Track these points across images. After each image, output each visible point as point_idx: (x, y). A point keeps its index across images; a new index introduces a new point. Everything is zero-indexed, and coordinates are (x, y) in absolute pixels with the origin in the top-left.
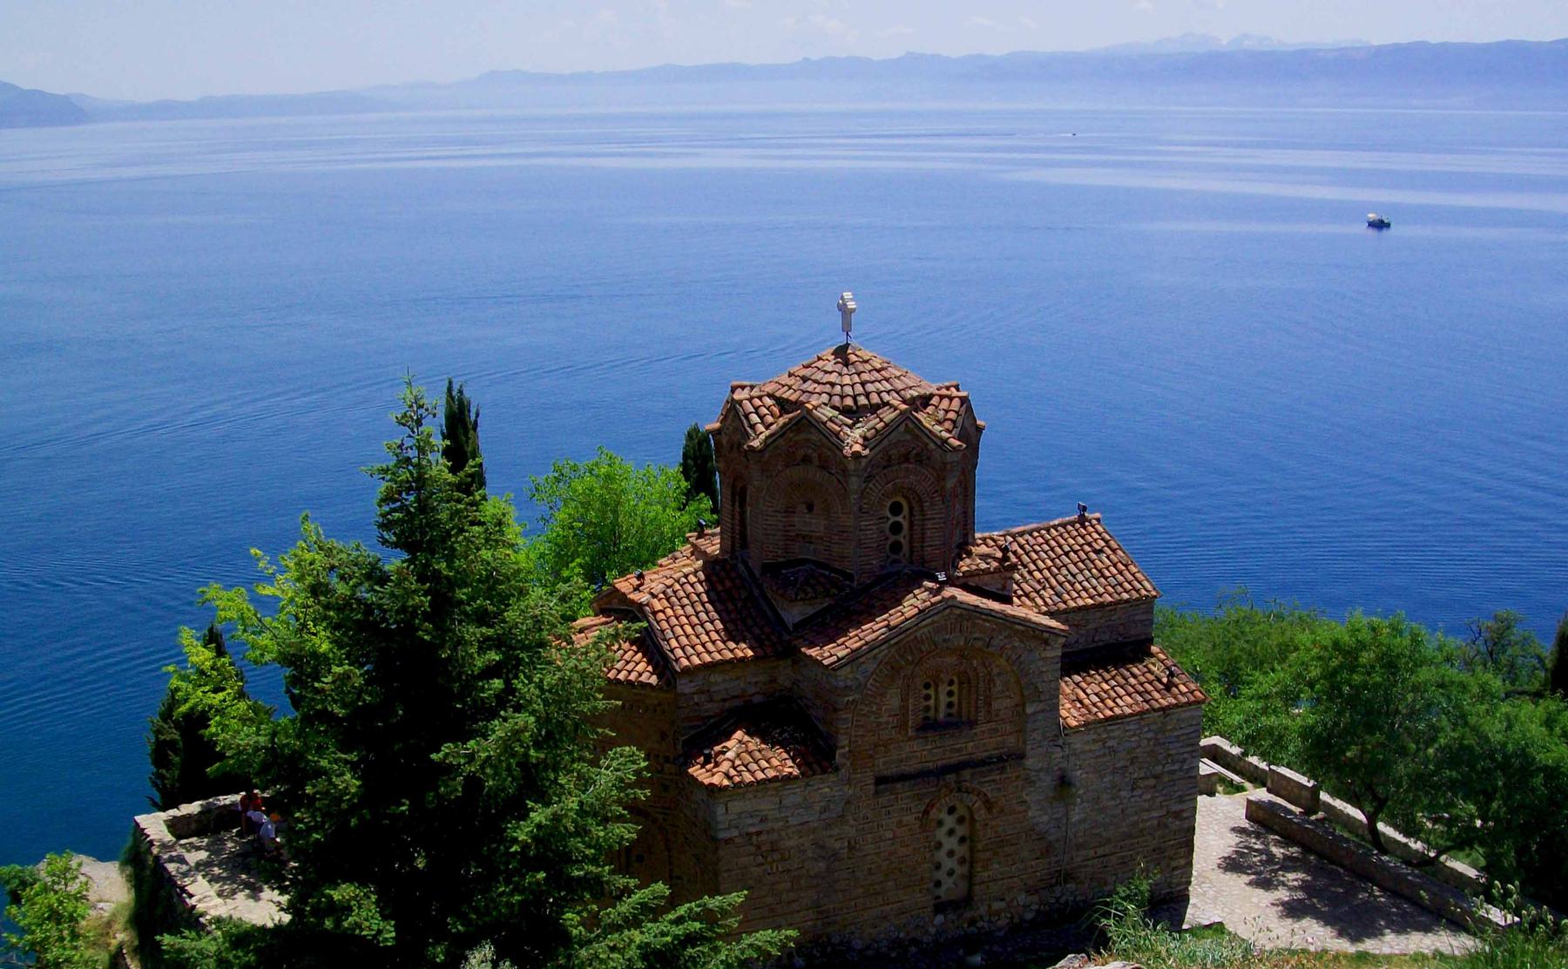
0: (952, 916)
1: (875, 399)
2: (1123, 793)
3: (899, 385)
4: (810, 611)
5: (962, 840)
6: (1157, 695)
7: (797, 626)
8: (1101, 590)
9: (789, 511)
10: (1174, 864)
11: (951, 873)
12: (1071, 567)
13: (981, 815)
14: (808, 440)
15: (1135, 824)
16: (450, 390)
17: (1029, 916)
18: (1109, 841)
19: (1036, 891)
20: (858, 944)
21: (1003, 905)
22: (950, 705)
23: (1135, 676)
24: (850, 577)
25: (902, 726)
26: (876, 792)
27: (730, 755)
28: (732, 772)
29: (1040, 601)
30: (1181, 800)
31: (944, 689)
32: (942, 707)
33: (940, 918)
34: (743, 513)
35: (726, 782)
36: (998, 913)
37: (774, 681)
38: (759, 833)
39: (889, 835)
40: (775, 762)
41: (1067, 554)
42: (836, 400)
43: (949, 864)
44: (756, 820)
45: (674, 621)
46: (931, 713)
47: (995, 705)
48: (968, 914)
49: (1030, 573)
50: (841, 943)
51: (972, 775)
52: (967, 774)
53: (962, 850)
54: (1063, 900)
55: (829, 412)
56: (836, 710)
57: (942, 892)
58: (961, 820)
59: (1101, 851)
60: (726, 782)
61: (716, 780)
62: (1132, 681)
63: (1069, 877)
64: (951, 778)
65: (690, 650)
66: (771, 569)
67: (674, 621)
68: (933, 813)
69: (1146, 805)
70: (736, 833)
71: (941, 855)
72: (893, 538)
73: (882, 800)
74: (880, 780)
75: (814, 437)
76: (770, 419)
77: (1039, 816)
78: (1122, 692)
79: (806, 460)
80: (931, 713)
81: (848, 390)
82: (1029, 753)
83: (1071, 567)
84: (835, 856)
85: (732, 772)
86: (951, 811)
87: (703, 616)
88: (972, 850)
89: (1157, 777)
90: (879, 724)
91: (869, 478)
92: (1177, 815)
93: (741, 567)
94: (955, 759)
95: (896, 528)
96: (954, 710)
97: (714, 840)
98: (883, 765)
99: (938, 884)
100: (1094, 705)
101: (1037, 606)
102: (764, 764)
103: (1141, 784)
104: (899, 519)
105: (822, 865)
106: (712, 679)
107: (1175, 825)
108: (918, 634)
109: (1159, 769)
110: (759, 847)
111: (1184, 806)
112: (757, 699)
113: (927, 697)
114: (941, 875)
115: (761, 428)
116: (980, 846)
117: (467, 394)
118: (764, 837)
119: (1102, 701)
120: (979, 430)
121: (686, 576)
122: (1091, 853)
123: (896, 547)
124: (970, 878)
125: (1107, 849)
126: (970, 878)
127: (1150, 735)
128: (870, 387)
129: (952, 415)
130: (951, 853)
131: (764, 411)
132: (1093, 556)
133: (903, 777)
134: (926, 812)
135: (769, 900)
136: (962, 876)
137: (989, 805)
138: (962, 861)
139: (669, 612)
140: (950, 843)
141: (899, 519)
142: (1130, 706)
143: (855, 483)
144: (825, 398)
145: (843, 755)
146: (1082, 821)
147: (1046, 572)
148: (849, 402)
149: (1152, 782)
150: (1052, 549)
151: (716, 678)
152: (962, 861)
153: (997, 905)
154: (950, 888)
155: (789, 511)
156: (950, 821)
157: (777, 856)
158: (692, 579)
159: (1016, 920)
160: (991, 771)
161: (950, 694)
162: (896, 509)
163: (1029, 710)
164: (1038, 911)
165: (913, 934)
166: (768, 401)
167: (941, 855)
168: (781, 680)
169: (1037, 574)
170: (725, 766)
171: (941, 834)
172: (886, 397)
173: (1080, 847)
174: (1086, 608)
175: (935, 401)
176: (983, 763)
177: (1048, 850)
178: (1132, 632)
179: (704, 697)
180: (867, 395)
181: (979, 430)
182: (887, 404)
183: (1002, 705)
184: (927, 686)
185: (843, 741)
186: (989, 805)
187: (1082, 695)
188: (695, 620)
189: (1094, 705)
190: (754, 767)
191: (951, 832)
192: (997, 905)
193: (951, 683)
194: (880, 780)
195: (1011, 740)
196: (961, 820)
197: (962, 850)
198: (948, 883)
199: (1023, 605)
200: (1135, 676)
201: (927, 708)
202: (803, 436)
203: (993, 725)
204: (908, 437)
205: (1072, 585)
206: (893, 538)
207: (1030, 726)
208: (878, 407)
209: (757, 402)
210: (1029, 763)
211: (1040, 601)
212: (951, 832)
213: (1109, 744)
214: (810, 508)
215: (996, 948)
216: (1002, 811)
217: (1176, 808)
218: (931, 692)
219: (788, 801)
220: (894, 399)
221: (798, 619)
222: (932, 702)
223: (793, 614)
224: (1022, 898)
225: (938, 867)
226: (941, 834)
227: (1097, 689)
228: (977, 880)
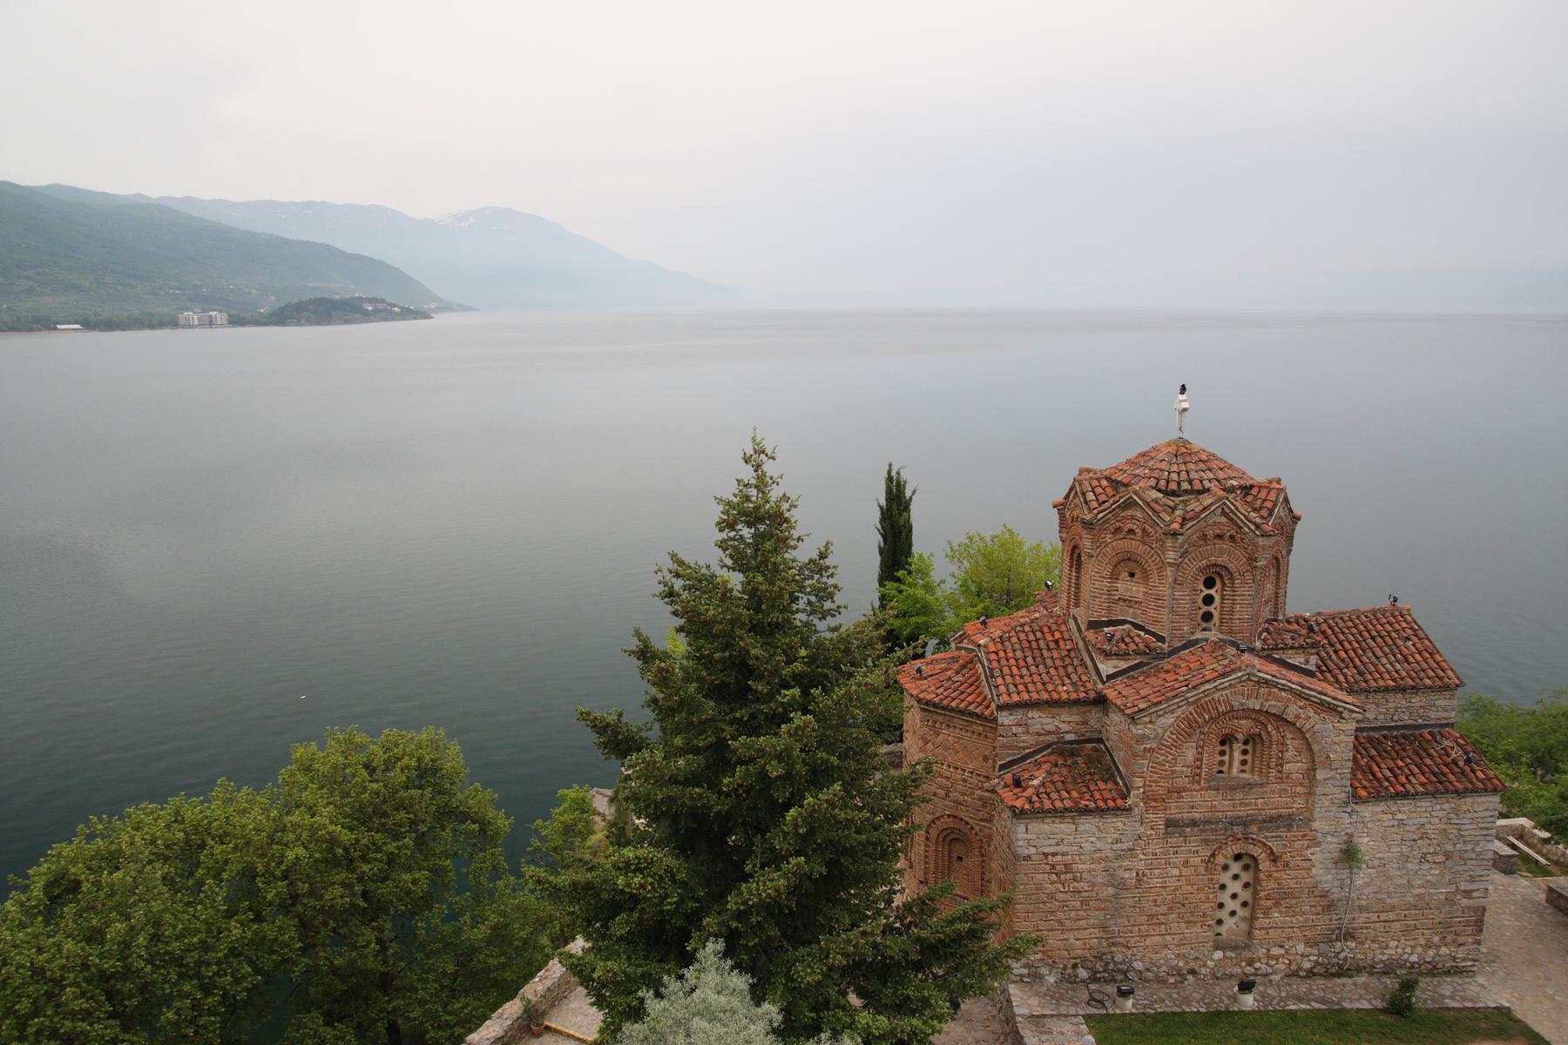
0: (1229, 954)
1: (1197, 486)
2: (1410, 866)
3: (1221, 475)
4: (1123, 665)
5: (1246, 885)
6: (1452, 777)
7: (1110, 677)
8: (1404, 674)
9: (1114, 577)
10: (1461, 940)
11: (1233, 913)
12: (1377, 651)
13: (1265, 865)
14: (1133, 517)
15: (1420, 896)
16: (889, 472)
17: (1307, 965)
18: (1393, 908)
19: (1316, 944)
20: (1138, 965)
21: (1282, 951)
22: (1244, 762)
23: (1429, 755)
24: (1162, 639)
25: (1195, 777)
26: (1167, 833)
27: (1035, 782)
28: (1035, 798)
29: (1342, 678)
30: (1472, 880)
31: (1238, 747)
32: (1236, 763)
33: (1218, 955)
34: (1078, 578)
35: (1027, 806)
36: (1277, 958)
37: (1085, 723)
38: (1054, 855)
39: (1176, 872)
40: (1075, 794)
41: (1373, 638)
42: (1163, 483)
43: (1231, 905)
44: (1053, 842)
45: (1003, 662)
46: (1225, 769)
47: (1287, 767)
48: (1246, 954)
49: (1336, 652)
50: (1124, 962)
51: (1260, 829)
52: (1254, 828)
53: (1245, 895)
54: (1342, 956)
55: (1155, 494)
56: (1135, 755)
57: (1223, 929)
58: (1246, 868)
59: (1383, 917)
60: (1027, 806)
61: (1018, 803)
62: (1428, 761)
63: (1349, 935)
64: (1238, 830)
65: (1012, 689)
66: (1095, 625)
67: (1003, 662)
68: (1220, 860)
69: (1433, 879)
70: (1033, 850)
71: (1225, 897)
72: (1205, 608)
73: (1173, 840)
74: (1170, 823)
75: (1139, 515)
76: (1102, 498)
77: (1323, 873)
78: (1416, 771)
79: (1131, 531)
80: (1225, 769)
81: (1175, 476)
82: (1317, 815)
83: (1377, 651)
84: (1122, 886)
85: (1035, 798)
86: (1238, 857)
87: (1030, 660)
88: (1255, 894)
89: (1448, 855)
90: (1173, 772)
91: (1184, 554)
92: (1468, 894)
93: (1071, 621)
94: (1242, 812)
95: (1208, 600)
96: (1247, 768)
97: (1015, 855)
98: (1176, 809)
99: (1220, 922)
100: (1387, 779)
101: (1337, 681)
102: (1064, 794)
103: (1429, 857)
104: (1212, 592)
105: (1111, 890)
106: (1030, 714)
107: (1465, 901)
108: (1216, 696)
109: (1449, 847)
110: (1053, 867)
111: (1473, 887)
112: (1069, 737)
113: (1222, 753)
114: (1224, 915)
115: (1095, 504)
116: (1262, 894)
117: (904, 476)
118: (1059, 858)
119: (1395, 776)
120: (1296, 519)
121: (1023, 625)
122: (1374, 917)
123: (1207, 617)
124: (1251, 919)
125: (1391, 916)
126: (1251, 919)
127: (1442, 814)
128: (1193, 475)
129: (1269, 505)
130: (1234, 896)
131: (1099, 490)
132: (1400, 643)
133: (1194, 823)
134: (1213, 855)
135: (1060, 915)
136: (1243, 919)
137: (1274, 858)
138: (1245, 904)
139: (1002, 654)
140: (1235, 887)
141: (1212, 592)
142: (1422, 784)
143: (1171, 556)
144: (1153, 482)
145: (1137, 796)
146: (1368, 885)
147: (1351, 653)
148: (1173, 486)
149: (1441, 858)
150: (1360, 633)
151: (1034, 714)
152: (1245, 904)
153: (1276, 951)
155: (1114, 577)
156: (1235, 868)
157: (1069, 876)
158: (1027, 628)
159: (1293, 967)
160: (1278, 827)
161: (1245, 752)
162: (1209, 583)
163: (1320, 775)
164: (1317, 963)
165: (1192, 965)
166: (1105, 483)
167: (1225, 897)
168: (1092, 722)
169: (1342, 654)
170: (1029, 792)
171: (1225, 878)
172: (1207, 484)
173: (1360, 908)
174: (1387, 690)
175: (1254, 491)
176: (1272, 819)
177: (1330, 907)
178: (1432, 714)
179: (1020, 730)
180: (1190, 482)
181: (1296, 519)
182: (1208, 490)
184: (1222, 743)
185: (1138, 782)
186: (1274, 858)
187: (1376, 769)
188: (1021, 663)
189: (1387, 779)
190: (1054, 796)
191: (1236, 877)
192: (1276, 951)
193: (1246, 742)
194: (1170, 823)
195: (1299, 803)
196: (1246, 868)
197: (1245, 895)
198: (1230, 923)
199: (1325, 680)
200: (1429, 755)
201: (1222, 763)
202: (1129, 513)
203: (1284, 786)
204: (1224, 520)
205: (1375, 666)
206: (1205, 608)
207: (1319, 790)
208: (1199, 492)
209: (1095, 483)
210: (1316, 825)
211: (1342, 678)
212: (1236, 877)
213: (1399, 816)
214: (1132, 575)
215: (1271, 992)
216: (1286, 865)
217: (1464, 886)
218: (1226, 748)
219: (1081, 828)
220: (1214, 486)
221: (1111, 671)
222: (1226, 758)
224: (1301, 948)
225: (1221, 906)
226: (1225, 878)
227: (1391, 764)
228: (1257, 924)
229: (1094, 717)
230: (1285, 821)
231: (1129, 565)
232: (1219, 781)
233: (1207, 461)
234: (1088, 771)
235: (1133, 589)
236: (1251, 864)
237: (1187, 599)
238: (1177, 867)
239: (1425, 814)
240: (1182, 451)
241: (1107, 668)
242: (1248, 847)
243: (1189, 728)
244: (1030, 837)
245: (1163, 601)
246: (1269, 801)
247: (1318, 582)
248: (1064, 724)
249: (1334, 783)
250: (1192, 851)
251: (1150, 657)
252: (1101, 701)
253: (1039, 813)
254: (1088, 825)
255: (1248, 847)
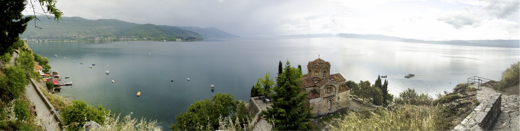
77: (337, 101)
154: (329, 108)
183: (334, 90)
223: (316, 82)
229: (315, 88)
230: (334, 96)
231: (317, 72)
232: (328, 93)
233: (322, 60)
234: (315, 93)
235: (317, 74)
236: (331, 101)
237: (322, 75)
238: (324, 102)
239: (344, 93)
240: (320, 60)
241: (316, 82)
242: (330, 98)
243: (325, 87)
244: (311, 101)
245: (320, 75)
246: (332, 94)
247: (332, 72)
248: (312, 89)
249: (337, 91)
250: (326, 100)
251: (320, 81)
252: (315, 86)
253: (311, 98)
254: (316, 99)
255: (330, 98)
